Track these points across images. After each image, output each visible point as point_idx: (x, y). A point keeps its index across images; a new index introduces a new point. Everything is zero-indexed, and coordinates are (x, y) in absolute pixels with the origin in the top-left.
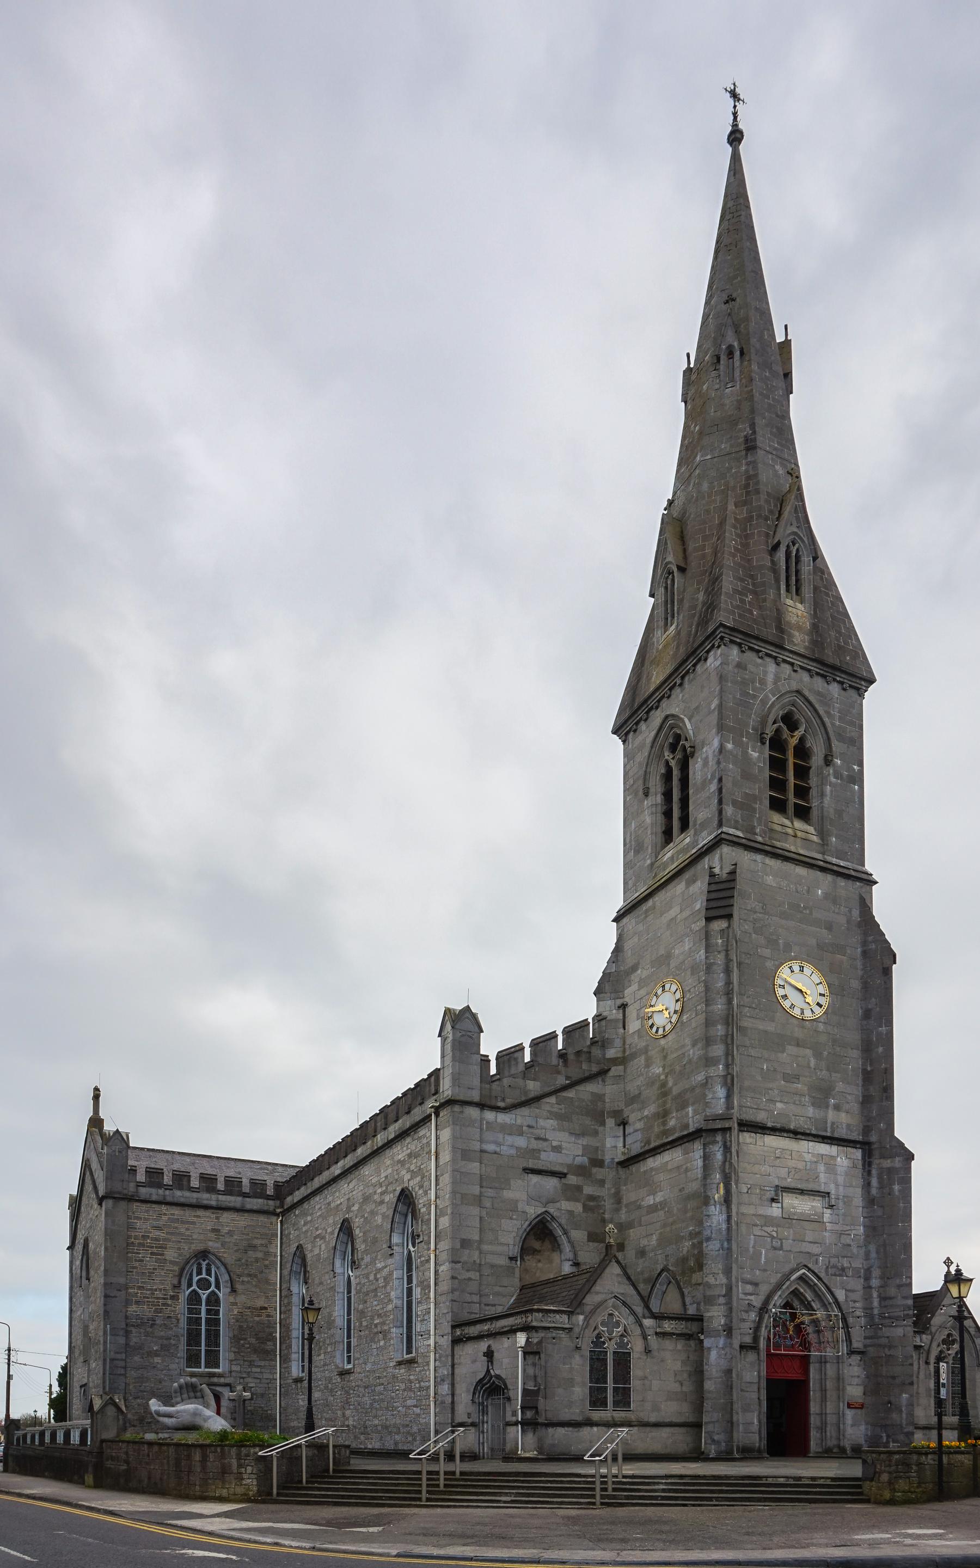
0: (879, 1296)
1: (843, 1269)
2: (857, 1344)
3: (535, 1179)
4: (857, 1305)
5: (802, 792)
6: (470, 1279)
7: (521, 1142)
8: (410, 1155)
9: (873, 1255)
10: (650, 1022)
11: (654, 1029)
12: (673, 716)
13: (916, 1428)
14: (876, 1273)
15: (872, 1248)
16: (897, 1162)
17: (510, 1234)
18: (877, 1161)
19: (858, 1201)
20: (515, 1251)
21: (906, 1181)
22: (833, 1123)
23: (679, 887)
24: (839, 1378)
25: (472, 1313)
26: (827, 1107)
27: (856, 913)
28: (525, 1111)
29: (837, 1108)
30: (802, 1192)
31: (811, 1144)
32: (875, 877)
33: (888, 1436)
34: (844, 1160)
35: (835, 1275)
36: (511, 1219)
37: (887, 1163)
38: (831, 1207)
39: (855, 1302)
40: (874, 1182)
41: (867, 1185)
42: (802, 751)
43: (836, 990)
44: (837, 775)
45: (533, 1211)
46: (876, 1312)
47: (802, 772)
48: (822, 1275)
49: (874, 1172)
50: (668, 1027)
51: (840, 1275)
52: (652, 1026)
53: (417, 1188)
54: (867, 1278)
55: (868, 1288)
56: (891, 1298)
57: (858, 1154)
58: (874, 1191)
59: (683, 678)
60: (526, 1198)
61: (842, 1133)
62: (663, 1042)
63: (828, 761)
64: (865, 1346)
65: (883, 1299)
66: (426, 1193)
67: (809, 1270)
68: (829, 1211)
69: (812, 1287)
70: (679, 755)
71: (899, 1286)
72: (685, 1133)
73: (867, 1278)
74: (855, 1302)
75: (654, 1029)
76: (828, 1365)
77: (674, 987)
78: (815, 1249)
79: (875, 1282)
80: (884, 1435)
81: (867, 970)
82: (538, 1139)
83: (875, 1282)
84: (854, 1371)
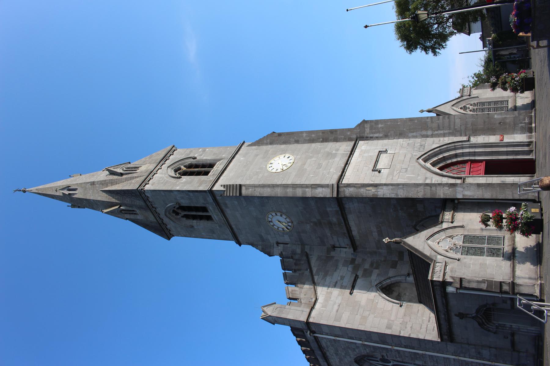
0: (437, 130)
5: (204, 166)
6: (411, 327)
8: (337, 354)
12: (165, 212)
14: (424, 133)
15: (410, 135)
23: (228, 212)
25: (433, 330)
26: (336, 154)
29: (337, 150)
30: (377, 161)
33: (521, 123)
39: (440, 141)
41: (377, 138)
42: (190, 166)
43: (284, 152)
44: (201, 155)
47: (197, 166)
48: (423, 153)
49: (371, 135)
50: (288, 220)
51: (424, 146)
53: (355, 353)
56: (439, 126)
58: (381, 135)
59: (153, 207)
63: (195, 158)
65: (439, 129)
66: (358, 347)
67: (420, 157)
70: (179, 211)
71: (432, 122)
72: (340, 212)
74: (440, 141)
77: (270, 216)
78: (409, 156)
80: (520, 125)
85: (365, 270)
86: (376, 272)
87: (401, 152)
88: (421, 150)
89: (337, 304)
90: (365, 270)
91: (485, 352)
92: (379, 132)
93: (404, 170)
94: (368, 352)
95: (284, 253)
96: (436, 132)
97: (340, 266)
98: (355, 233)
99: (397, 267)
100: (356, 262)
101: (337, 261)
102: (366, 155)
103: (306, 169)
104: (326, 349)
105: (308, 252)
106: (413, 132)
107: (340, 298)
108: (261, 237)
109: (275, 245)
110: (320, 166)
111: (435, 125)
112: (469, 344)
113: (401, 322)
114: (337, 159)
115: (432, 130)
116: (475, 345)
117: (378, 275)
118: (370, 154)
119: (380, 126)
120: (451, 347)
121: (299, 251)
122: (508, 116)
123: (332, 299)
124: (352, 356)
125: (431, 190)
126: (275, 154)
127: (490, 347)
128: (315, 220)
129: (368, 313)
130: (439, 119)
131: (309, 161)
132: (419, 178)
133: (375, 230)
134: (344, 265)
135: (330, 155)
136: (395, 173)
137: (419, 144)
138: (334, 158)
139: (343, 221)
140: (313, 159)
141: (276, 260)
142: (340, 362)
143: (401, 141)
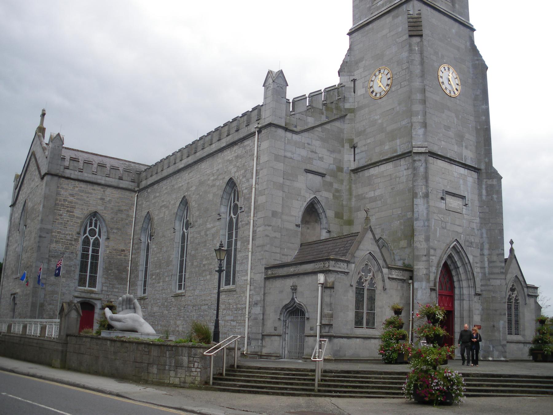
1: (471, 243)
2: (478, 290)
3: (310, 176)
4: (478, 265)
6: (275, 237)
7: (304, 153)
9: (485, 235)
10: (371, 90)
11: (374, 94)
13: (508, 342)
14: (486, 246)
15: (484, 231)
16: (495, 182)
17: (298, 209)
18: (485, 180)
19: (477, 203)
20: (299, 222)
21: (499, 192)
22: (465, 156)
24: (470, 310)
25: (275, 260)
26: (462, 146)
27: (468, 44)
28: (306, 134)
29: (466, 148)
30: (454, 195)
31: (457, 167)
32: (475, 27)
33: (493, 347)
34: (471, 177)
35: (468, 246)
36: (297, 200)
37: (490, 182)
38: (466, 205)
39: (477, 263)
40: (484, 192)
41: (480, 195)
45: (309, 197)
46: (487, 270)
48: (463, 245)
49: (484, 186)
51: (471, 247)
52: (372, 92)
53: (241, 178)
54: (482, 250)
55: (482, 255)
56: (494, 262)
57: (475, 175)
58: (484, 198)
60: (305, 188)
61: (469, 163)
62: (379, 101)
64: (481, 291)
65: (490, 262)
66: (248, 180)
67: (458, 242)
68: (465, 207)
69: (458, 253)
71: (498, 255)
73: (482, 250)
74: (477, 263)
75: (374, 94)
76: (464, 302)
78: (460, 230)
79: (486, 252)
80: (491, 346)
81: (476, 72)
82: (312, 152)
83: (486, 252)
84: (477, 306)
85: (331, 184)
86: (330, 196)
87: (465, 221)
88: (467, 244)
89: (292, 156)
90: (331, 184)
91: (257, 310)
92: (488, 195)
93: (444, 226)
94: (244, 192)
95: (343, 88)
96: (486, 259)
97: (334, 155)
98: (374, 171)
99: (336, 219)
100: (339, 173)
101: (340, 152)
102: (461, 182)
103: (443, 113)
104: (242, 145)
105: (348, 117)
106: (487, 234)
107: (299, 158)
108: (361, 60)
109: (352, 78)
110: (448, 128)
111: (495, 258)
112: (264, 294)
113: (280, 226)
114: (456, 148)
115: (489, 255)
116: (264, 300)
117: (327, 198)
118: (462, 186)
119: (495, 196)
120: (260, 277)
121: (347, 106)
122: (501, 334)
123: (297, 149)
124: (237, 174)
125: (423, 255)
126: (460, 72)
127: (263, 314)
128: (385, 125)
129: (286, 190)
130: (501, 262)
131: (453, 115)
132: (436, 242)
133: (377, 194)
134: (335, 159)
135: (460, 138)
136: (440, 216)
137: (473, 240)
138: (457, 144)
139: (385, 158)
140: (455, 119)
141: (335, 80)
142: (228, 160)
143: (478, 220)
